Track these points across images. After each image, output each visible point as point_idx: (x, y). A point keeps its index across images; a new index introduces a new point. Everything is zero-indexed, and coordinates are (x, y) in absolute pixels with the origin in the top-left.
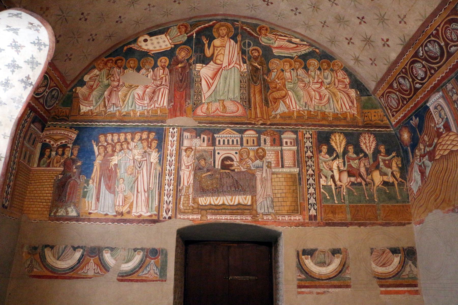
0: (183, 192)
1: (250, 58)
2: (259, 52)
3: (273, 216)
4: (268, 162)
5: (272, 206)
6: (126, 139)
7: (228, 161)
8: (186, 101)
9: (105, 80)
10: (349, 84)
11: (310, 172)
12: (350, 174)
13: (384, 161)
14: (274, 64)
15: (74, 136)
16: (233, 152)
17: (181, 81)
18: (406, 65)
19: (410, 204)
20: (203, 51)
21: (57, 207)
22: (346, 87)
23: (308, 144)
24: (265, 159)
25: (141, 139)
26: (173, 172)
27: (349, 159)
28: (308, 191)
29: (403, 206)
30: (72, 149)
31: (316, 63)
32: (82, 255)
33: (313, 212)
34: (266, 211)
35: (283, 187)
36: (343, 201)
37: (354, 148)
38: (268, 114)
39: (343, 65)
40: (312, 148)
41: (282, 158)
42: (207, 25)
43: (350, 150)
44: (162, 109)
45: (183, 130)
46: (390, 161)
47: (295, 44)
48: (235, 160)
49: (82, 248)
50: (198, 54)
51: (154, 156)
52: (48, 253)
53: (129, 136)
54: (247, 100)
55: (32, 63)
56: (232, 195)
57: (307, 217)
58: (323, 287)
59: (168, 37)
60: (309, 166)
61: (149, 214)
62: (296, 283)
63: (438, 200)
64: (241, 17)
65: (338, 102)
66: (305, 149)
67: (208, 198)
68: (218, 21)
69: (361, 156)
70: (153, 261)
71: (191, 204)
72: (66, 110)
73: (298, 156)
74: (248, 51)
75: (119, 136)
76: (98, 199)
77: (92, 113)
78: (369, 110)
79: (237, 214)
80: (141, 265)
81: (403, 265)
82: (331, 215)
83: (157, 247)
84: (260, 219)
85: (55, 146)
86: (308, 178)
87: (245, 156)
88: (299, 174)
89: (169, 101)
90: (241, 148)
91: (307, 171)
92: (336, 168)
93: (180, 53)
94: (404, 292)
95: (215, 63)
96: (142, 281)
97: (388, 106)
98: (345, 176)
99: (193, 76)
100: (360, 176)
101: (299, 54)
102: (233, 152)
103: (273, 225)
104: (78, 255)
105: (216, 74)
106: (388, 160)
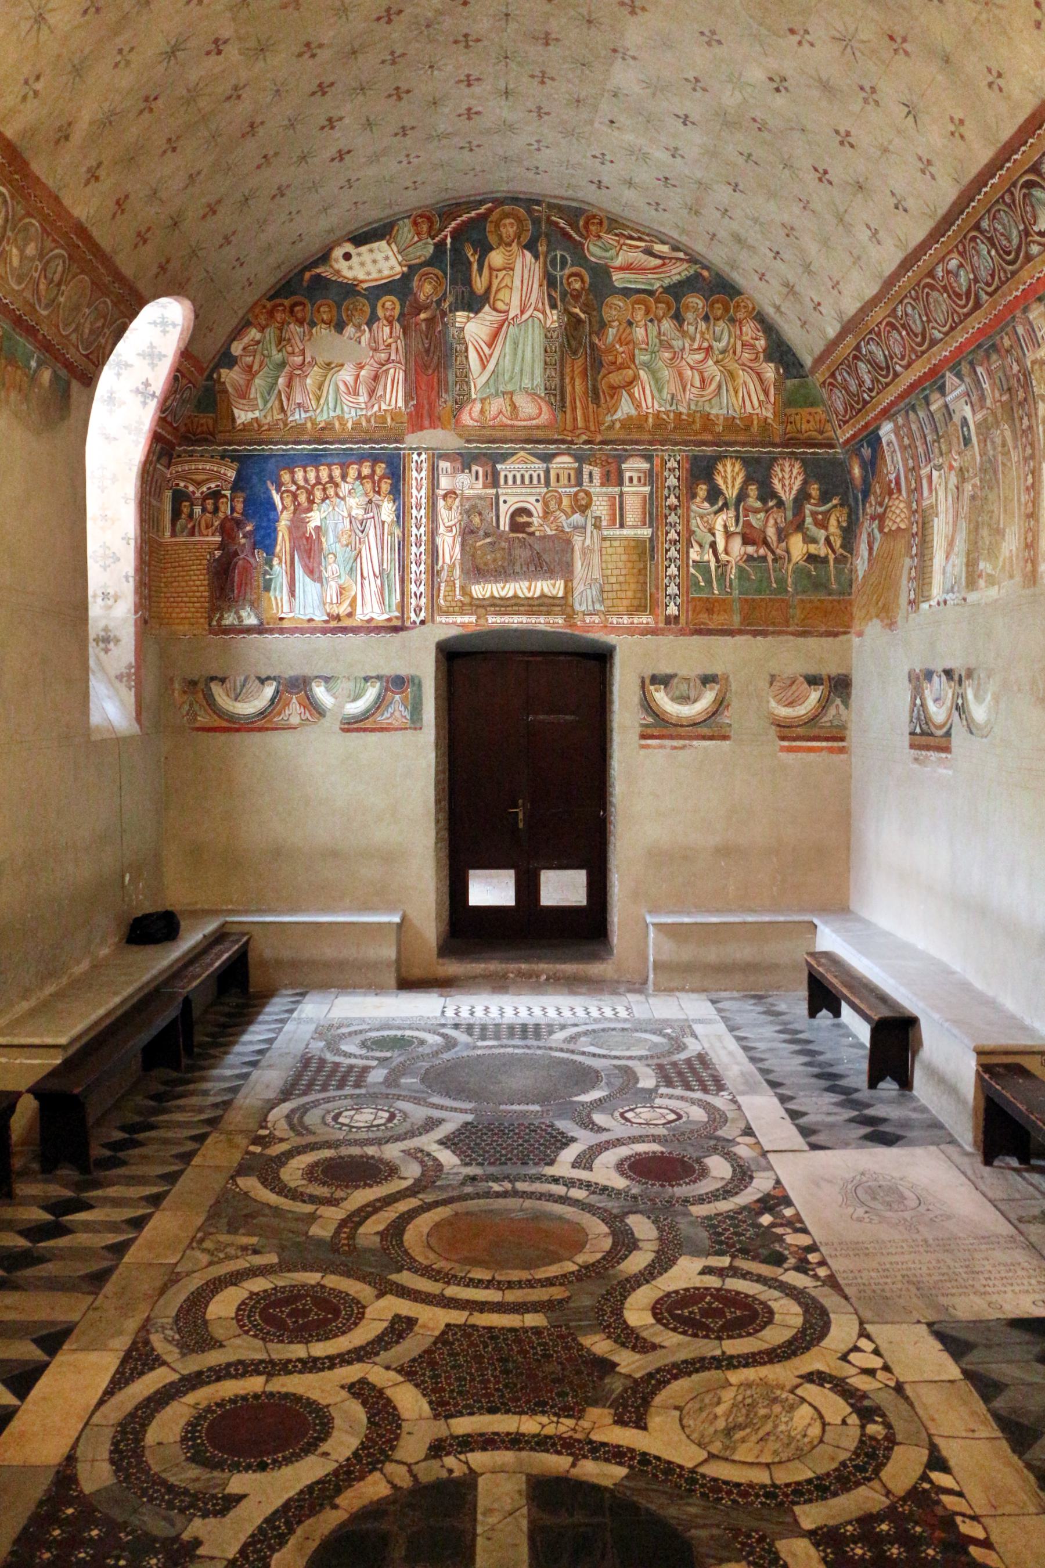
0: (444, 575)
1: (564, 295)
2: (583, 281)
4: (596, 518)
6: (331, 477)
8: (439, 396)
9: (274, 352)
10: (764, 351)
11: (673, 535)
12: (746, 541)
13: (814, 514)
14: (615, 308)
15: (232, 474)
16: (532, 499)
17: (428, 351)
20: (468, 282)
21: (220, 609)
22: (757, 358)
23: (672, 481)
25: (360, 477)
26: (424, 538)
29: (839, 602)
30: (232, 500)
31: (700, 306)
32: (277, 692)
33: (672, 610)
35: (620, 565)
41: (621, 509)
42: (473, 214)
43: (752, 493)
44: (395, 415)
45: (437, 456)
47: (660, 257)
49: (274, 679)
50: (460, 288)
51: (387, 510)
52: (216, 689)
53: (337, 472)
54: (558, 392)
55: (151, 355)
56: (530, 580)
57: (662, 618)
58: (680, 737)
59: (393, 246)
61: (386, 616)
62: (638, 730)
64: (545, 196)
65: (736, 392)
66: (666, 492)
67: (488, 586)
68: (499, 202)
69: (771, 504)
70: (397, 697)
71: (458, 597)
72: (206, 420)
73: (651, 504)
74: (561, 277)
75: (318, 471)
76: (292, 593)
77: (260, 426)
78: (799, 410)
79: (539, 613)
80: (379, 703)
81: (824, 704)
82: (704, 617)
83: (403, 672)
85: (198, 495)
87: (553, 505)
88: (651, 539)
89: (408, 397)
90: (545, 490)
91: (667, 533)
92: (721, 529)
93: (420, 287)
94: (821, 749)
95: (495, 309)
96: (382, 730)
98: (736, 544)
99: (451, 339)
100: (765, 543)
102: (532, 499)
104: (269, 691)
105: (495, 335)
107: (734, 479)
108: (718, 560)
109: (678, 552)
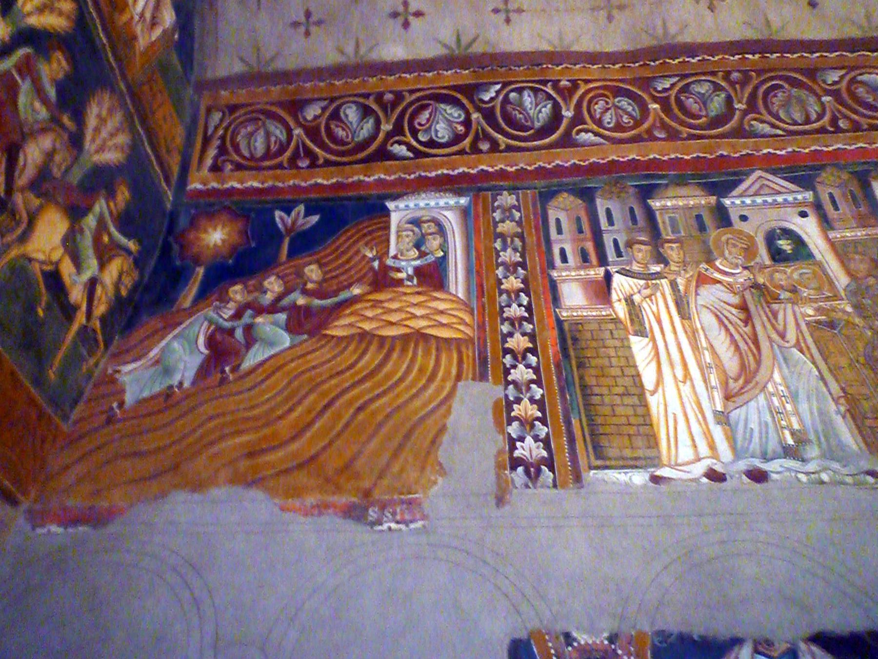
13: (102, 225)
18: (412, 92)
19: (65, 427)
29: (41, 415)
37: (67, 76)
43: (55, 65)
46: (116, 248)
63: (270, 457)
69: (66, 120)
97: (223, 138)
106: (110, 235)
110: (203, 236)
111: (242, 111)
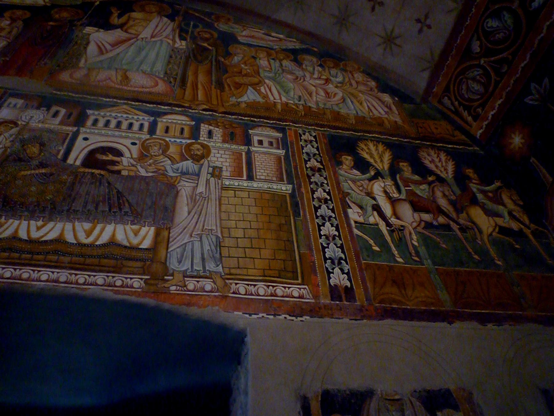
3: (219, 282)
4: (214, 168)
5: (218, 256)
7: (107, 155)
10: (377, 87)
16: (128, 142)
24: (206, 161)
27: (407, 182)
28: (320, 230)
34: (198, 267)
35: (250, 217)
36: (416, 259)
38: (221, 100)
39: (362, 68)
40: (320, 156)
43: (405, 169)
46: (496, 191)
48: (127, 154)
57: (324, 290)
60: (316, 184)
65: (361, 104)
69: (430, 179)
84: (173, 288)
86: (317, 206)
87: (155, 150)
88: (292, 195)
91: (313, 192)
97: (460, 104)
98: (406, 210)
100: (440, 211)
101: (284, 47)
102: (128, 142)
103: (217, 308)
107: (381, 157)
108: (388, 224)
109: (333, 210)
110: (512, 147)
111: (452, 87)
